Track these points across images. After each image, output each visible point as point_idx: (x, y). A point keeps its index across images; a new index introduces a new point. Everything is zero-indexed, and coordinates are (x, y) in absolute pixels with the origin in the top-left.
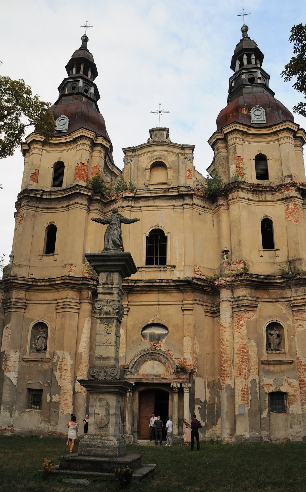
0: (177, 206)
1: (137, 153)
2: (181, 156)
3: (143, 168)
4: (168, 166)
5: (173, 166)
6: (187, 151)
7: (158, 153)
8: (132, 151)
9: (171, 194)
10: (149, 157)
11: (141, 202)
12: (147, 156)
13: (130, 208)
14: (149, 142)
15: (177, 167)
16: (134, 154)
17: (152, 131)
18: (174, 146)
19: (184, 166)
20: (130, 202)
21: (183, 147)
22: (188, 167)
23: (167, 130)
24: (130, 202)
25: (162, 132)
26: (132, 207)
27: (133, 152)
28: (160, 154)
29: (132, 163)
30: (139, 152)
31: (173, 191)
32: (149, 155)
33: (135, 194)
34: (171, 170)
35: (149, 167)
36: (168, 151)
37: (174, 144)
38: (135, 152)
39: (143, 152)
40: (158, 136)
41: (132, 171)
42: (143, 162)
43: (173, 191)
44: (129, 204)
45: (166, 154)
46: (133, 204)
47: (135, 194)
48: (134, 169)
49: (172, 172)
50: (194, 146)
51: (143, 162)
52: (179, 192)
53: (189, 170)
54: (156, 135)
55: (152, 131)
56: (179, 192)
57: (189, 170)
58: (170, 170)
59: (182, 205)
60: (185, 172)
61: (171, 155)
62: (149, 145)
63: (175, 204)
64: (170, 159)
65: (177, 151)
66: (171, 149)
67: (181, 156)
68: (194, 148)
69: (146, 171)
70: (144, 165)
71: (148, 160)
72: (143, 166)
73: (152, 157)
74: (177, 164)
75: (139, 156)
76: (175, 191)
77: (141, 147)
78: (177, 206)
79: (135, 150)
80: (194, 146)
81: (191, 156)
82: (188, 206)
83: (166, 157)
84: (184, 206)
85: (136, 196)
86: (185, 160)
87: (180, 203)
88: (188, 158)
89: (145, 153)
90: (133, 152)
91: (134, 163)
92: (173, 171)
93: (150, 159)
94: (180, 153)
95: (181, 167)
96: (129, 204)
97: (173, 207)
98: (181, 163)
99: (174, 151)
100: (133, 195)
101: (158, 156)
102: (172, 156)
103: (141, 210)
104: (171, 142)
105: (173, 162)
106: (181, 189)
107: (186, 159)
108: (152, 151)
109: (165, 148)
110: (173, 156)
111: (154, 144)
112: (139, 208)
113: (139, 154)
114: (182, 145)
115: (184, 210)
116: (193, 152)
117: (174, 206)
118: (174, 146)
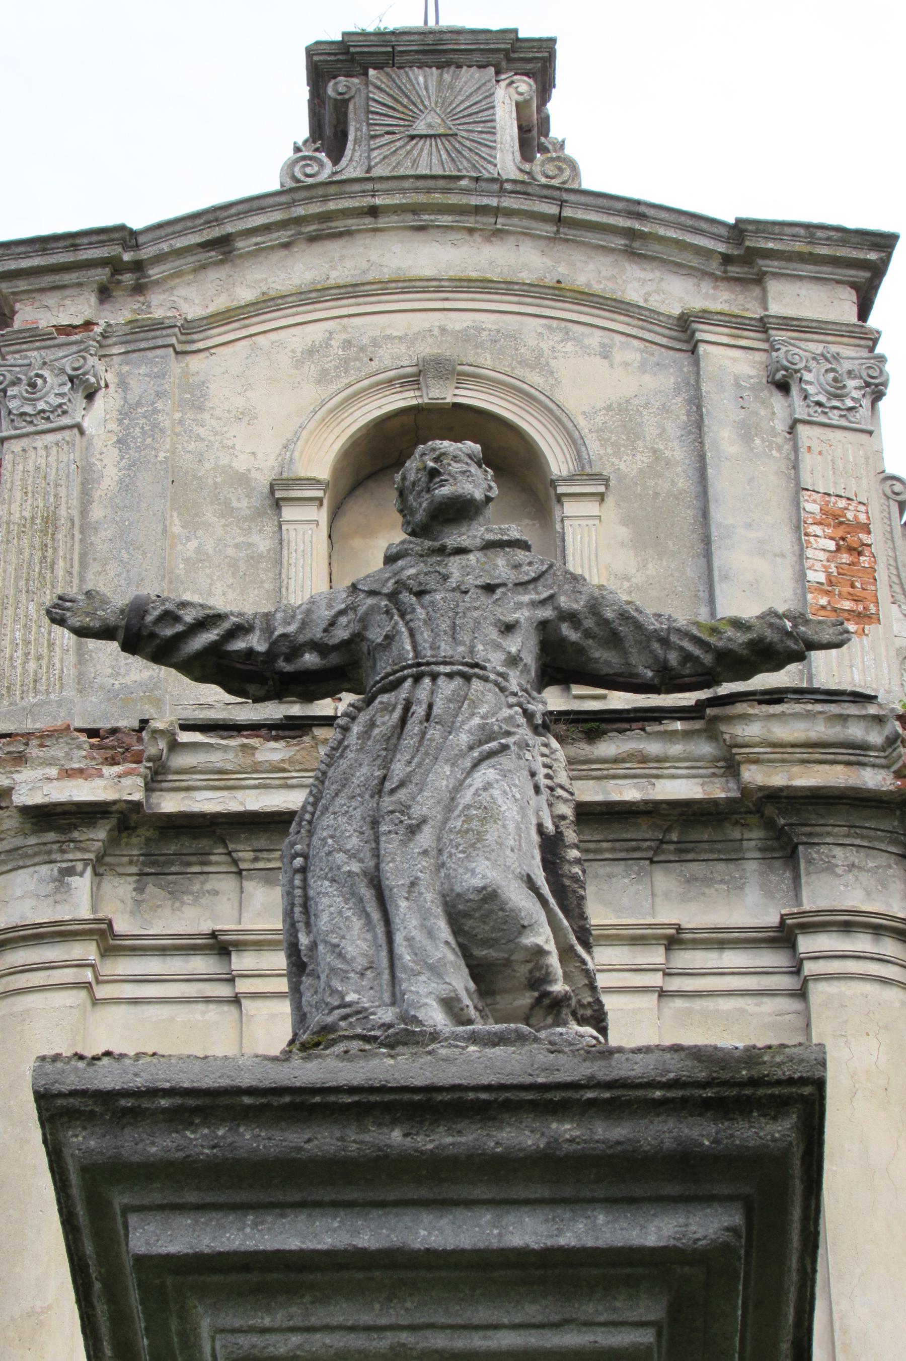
0: (720, 940)
1: (158, 306)
2: (730, 363)
3: (243, 480)
4: (558, 461)
5: (627, 465)
6: (791, 298)
7: (416, 313)
8: (101, 275)
9: (629, 792)
10: (311, 352)
11: (226, 885)
12: (298, 339)
13: (88, 951)
14: (295, 190)
15: (681, 480)
16: (120, 313)
17: (342, 70)
18: (631, 234)
19: (770, 474)
20: (82, 884)
21: (746, 252)
22: (817, 472)
23: (532, 60)
24: (82, 884)
25: (470, 78)
26: (105, 938)
27: (104, 293)
28: (457, 322)
29: (98, 418)
30: (189, 298)
31: (654, 748)
32: (316, 333)
33: (149, 788)
34: (610, 510)
35: (324, 473)
36: (557, 292)
37: (635, 209)
38: (139, 289)
39: (245, 295)
40: (420, 127)
41: (97, 513)
42: (246, 416)
43: (654, 748)
44: (80, 900)
45: (531, 330)
46: (119, 903)
47: (157, 777)
48: (126, 485)
49: (624, 533)
50: (885, 243)
51: (246, 416)
52: (730, 765)
53: (833, 518)
54: (407, 108)
55: (342, 70)
56: (730, 765)
57: (833, 518)
58: (590, 508)
59: (784, 937)
60: (784, 540)
61: (595, 339)
62: (302, 214)
63: (670, 914)
64: (583, 384)
65: (676, 294)
66: (590, 271)
67: (730, 363)
68: (878, 271)
69: (288, 513)
70: (257, 454)
71: (311, 393)
72: (241, 464)
73: (358, 351)
74: (678, 452)
75: (188, 336)
76: (676, 749)
77: (216, 237)
78: (720, 940)
79: (138, 266)
80: (885, 243)
81: (850, 354)
82: (862, 943)
83: (538, 363)
84: (806, 944)
85: (170, 804)
86: (777, 400)
87: (753, 904)
88: (814, 381)
89: (268, 304)
90: (104, 293)
91: (126, 413)
92: (627, 520)
93: (323, 377)
94: (705, 316)
95: (725, 483)
96: (80, 900)
97: (656, 956)
98: (723, 436)
99: (634, 294)
100: (131, 789)
101: (426, 349)
102: (606, 354)
103: (223, 990)
104: (588, 183)
105: (625, 418)
106: (750, 731)
107: (783, 387)
108: (352, 291)
109: (523, 259)
110: (629, 353)
111: (374, 212)
112: (200, 964)
113: (194, 311)
114: (740, 230)
115: (801, 994)
116: (864, 311)
117: (674, 940)
118: (636, 230)
